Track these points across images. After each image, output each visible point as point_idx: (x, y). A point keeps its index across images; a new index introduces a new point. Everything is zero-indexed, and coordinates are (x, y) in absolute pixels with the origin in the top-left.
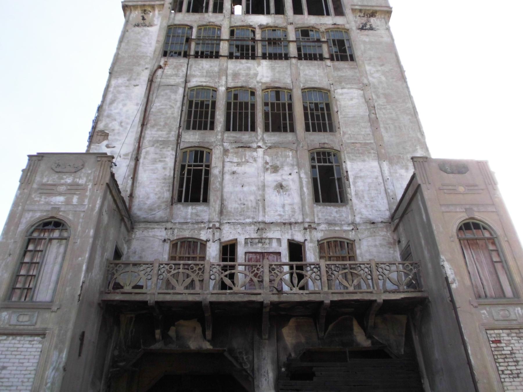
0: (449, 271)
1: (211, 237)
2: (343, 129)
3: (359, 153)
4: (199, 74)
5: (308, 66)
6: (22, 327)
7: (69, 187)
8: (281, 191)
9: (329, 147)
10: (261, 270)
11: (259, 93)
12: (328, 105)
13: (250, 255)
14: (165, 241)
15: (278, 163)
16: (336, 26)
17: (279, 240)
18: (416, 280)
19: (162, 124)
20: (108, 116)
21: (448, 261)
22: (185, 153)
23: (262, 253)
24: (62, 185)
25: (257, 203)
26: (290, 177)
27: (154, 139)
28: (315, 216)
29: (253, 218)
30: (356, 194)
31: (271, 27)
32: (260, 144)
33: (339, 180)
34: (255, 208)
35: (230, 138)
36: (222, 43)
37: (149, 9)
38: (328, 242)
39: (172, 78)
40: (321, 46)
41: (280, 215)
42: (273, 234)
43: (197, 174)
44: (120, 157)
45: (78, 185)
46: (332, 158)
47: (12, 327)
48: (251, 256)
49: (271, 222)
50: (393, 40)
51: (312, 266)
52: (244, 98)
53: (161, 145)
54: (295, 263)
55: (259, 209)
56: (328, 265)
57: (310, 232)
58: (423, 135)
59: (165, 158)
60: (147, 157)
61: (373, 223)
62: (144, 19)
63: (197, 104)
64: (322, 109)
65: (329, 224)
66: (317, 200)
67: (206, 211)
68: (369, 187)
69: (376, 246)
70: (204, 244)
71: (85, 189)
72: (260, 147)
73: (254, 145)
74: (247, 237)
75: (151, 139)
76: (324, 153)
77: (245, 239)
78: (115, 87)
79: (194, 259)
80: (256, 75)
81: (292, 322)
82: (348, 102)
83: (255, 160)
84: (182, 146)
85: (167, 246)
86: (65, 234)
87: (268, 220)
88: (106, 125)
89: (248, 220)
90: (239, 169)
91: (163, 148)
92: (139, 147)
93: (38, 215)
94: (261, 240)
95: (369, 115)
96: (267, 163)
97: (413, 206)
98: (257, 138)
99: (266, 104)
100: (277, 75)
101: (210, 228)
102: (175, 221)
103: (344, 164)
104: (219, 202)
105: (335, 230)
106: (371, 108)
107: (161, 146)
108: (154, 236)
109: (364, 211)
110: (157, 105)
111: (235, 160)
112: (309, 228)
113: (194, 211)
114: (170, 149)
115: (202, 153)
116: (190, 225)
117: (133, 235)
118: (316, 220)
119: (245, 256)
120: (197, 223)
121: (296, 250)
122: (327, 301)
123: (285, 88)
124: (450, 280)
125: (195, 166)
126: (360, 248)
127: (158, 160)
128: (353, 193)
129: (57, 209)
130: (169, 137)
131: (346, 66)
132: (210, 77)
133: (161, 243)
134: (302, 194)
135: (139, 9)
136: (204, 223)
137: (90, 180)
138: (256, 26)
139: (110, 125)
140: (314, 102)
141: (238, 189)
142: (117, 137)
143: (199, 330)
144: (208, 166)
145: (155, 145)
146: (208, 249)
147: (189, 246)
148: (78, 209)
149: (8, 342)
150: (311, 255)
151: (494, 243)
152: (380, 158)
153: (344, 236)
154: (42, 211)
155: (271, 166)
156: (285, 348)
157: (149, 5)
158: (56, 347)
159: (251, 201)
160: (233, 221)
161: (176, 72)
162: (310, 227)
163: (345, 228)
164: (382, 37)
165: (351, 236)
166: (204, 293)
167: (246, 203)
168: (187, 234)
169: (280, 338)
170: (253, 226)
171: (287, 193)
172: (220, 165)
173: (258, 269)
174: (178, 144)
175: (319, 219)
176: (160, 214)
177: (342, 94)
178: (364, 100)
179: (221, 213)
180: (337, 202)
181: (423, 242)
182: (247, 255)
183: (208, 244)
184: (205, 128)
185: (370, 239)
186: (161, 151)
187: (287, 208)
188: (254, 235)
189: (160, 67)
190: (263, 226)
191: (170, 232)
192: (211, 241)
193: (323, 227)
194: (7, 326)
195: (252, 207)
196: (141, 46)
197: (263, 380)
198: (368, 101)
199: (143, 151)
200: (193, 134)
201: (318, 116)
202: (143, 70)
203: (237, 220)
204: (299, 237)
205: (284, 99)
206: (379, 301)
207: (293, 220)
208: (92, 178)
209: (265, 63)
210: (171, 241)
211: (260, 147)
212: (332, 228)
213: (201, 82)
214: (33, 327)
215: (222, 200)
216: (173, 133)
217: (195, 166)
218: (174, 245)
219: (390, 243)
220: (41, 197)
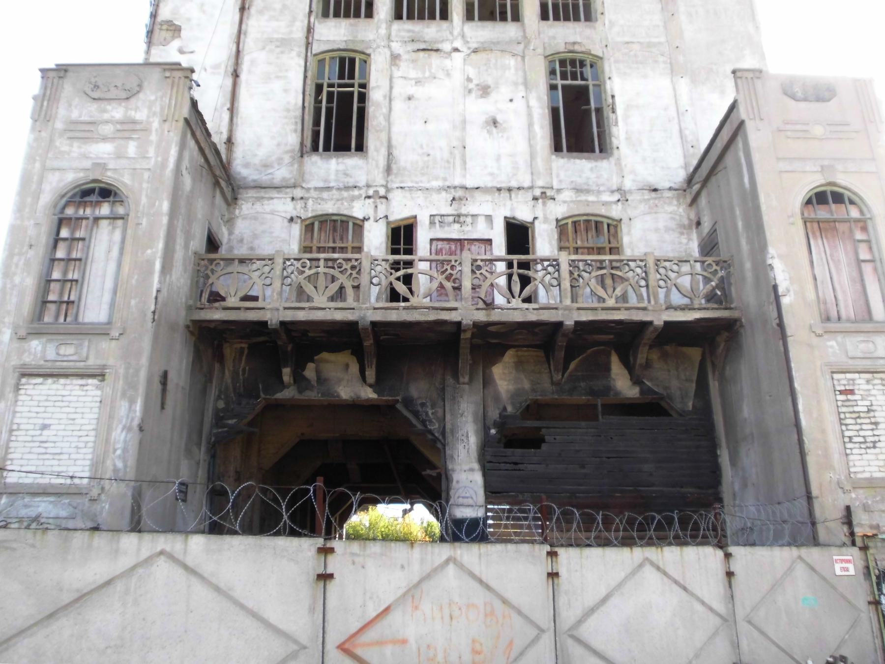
0: (781, 275)
1: (370, 212)
2: (609, 16)
6: (65, 364)
7: (119, 127)
8: (494, 130)
9: (583, 49)
10: (459, 268)
13: (440, 243)
14: (291, 220)
15: (490, 81)
17: (489, 218)
18: (723, 289)
19: (278, 6)
21: (780, 257)
22: (321, 62)
23: (460, 240)
24: (107, 122)
25: (451, 153)
28: (554, 175)
29: (445, 179)
30: (628, 139)
32: (458, 44)
33: (599, 111)
34: (448, 162)
35: (403, 34)
38: (574, 223)
41: (491, 174)
42: (478, 206)
43: (345, 99)
44: (206, 70)
45: (134, 122)
46: (588, 71)
47: (49, 364)
48: (440, 245)
49: (476, 186)
51: (546, 263)
53: (277, 47)
54: (516, 258)
55: (454, 163)
56: (573, 261)
57: (544, 204)
59: (287, 71)
61: (655, 190)
65: (578, 190)
66: (557, 148)
69: (657, 230)
70: (359, 226)
71: (147, 130)
72: (456, 50)
73: (447, 47)
76: (573, 62)
77: (431, 216)
79: (343, 250)
81: (509, 356)
83: (448, 75)
84: (316, 48)
85: (296, 229)
86: (121, 210)
87: (470, 183)
89: (436, 184)
91: (282, 52)
92: (238, 52)
94: (458, 218)
96: (469, 80)
97: (729, 159)
98: (451, 33)
101: (369, 197)
102: (309, 186)
103: (608, 82)
104: (384, 151)
105: (587, 201)
107: (278, 50)
108: (272, 213)
111: (413, 74)
112: (542, 198)
113: (341, 167)
114: (294, 54)
115: (352, 61)
116: (334, 192)
117: (237, 212)
118: (556, 185)
119: (431, 245)
120: (347, 188)
121: (518, 236)
122: (569, 323)
124: (781, 290)
125: (340, 86)
126: (629, 233)
130: (291, 32)
133: (286, 223)
134: (531, 139)
136: (360, 188)
137: (155, 114)
143: (355, 368)
144: (363, 86)
145: (267, 48)
146: (366, 233)
147: (335, 230)
148: (138, 166)
149: (46, 387)
150: (544, 243)
151: (864, 229)
152: (674, 70)
153: (603, 211)
154: (76, 170)
155: (478, 85)
156: (497, 398)
158: (124, 395)
159: (441, 149)
160: (410, 185)
162: (544, 196)
163: (606, 197)
165: (615, 212)
166: (361, 309)
167: (431, 152)
168: (329, 208)
169: (488, 381)
170: (444, 194)
172: (385, 84)
173: (452, 267)
174: (308, 45)
175: (560, 181)
176: (281, 173)
179: (388, 170)
180: (593, 151)
181: (740, 224)
182: (434, 243)
183: (367, 225)
184: (357, 15)
185: (648, 218)
186: (278, 58)
188: (447, 210)
190: (461, 194)
191: (300, 204)
192: (372, 219)
193: (567, 195)
194: (42, 362)
195: (442, 159)
197: (460, 447)
200: (335, 26)
203: (417, 183)
204: (523, 214)
206: (656, 323)
207: (514, 184)
210: (303, 221)
211: (456, 50)
212: (583, 197)
214: (82, 364)
215: (390, 147)
217: (340, 86)
218: (308, 228)
219: (683, 226)
220: (72, 146)
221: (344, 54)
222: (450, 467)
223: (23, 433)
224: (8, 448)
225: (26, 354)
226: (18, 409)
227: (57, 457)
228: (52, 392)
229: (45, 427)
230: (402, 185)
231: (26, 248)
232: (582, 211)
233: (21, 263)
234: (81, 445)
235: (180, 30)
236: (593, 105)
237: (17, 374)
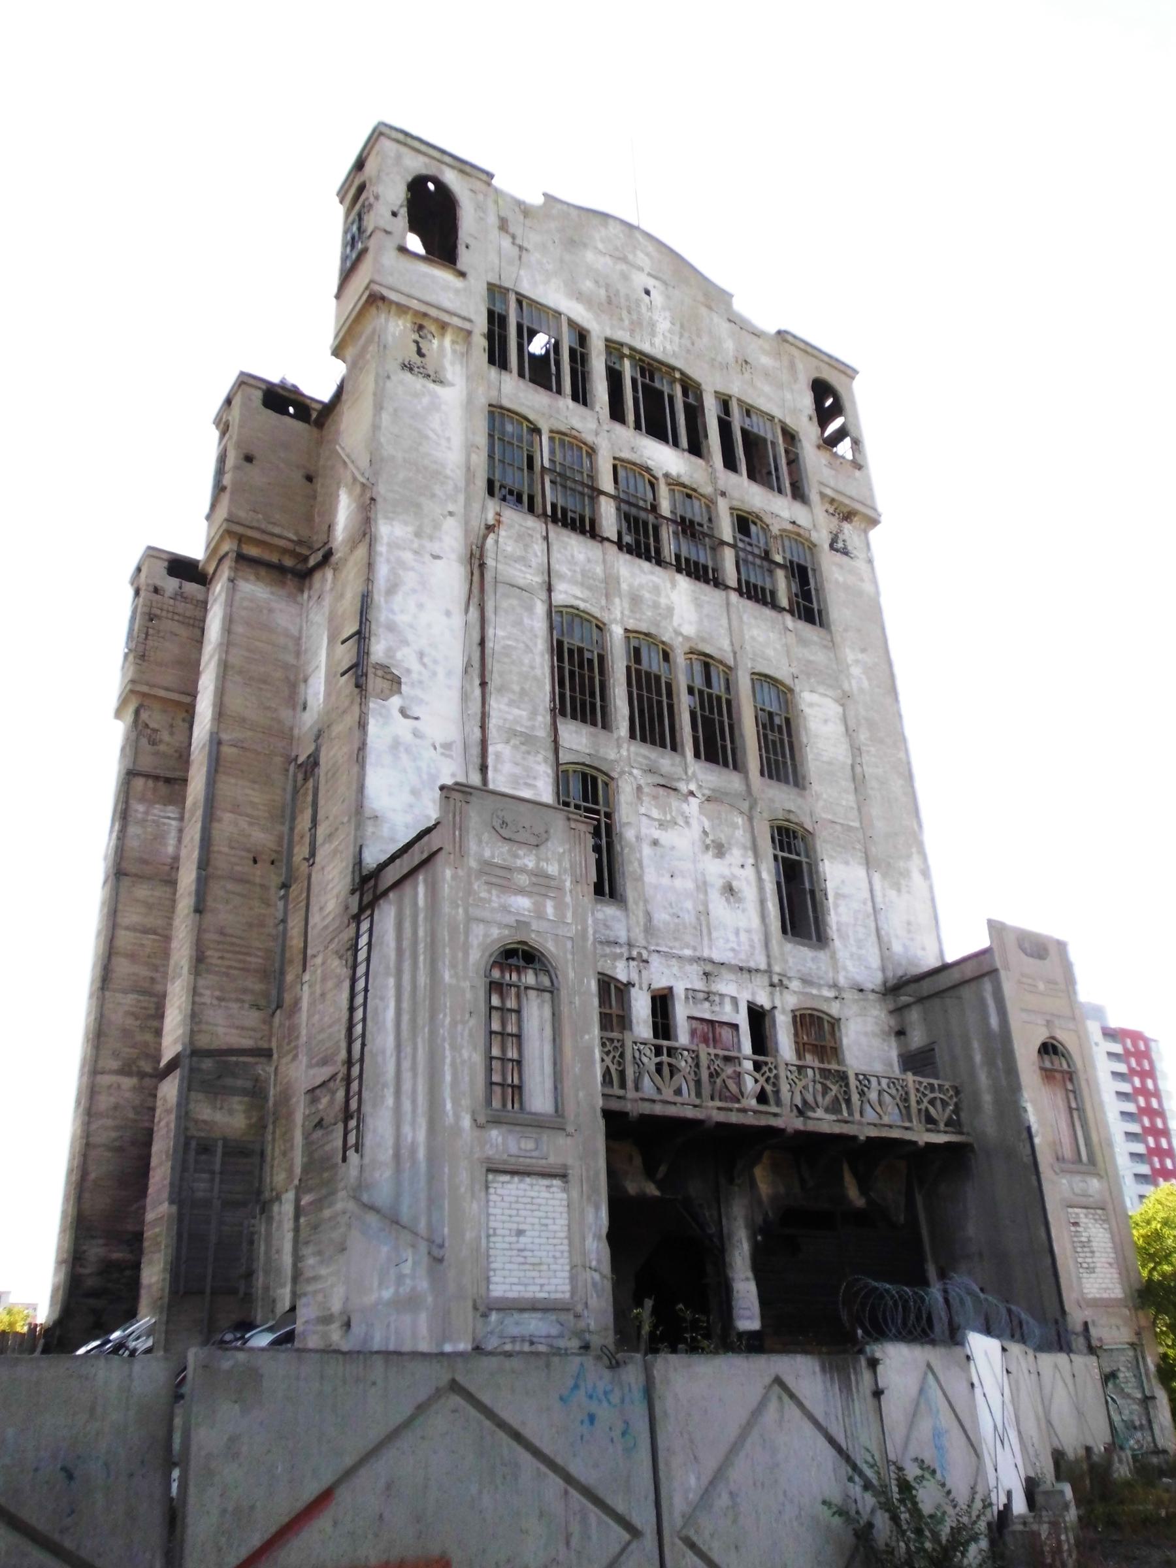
0: (1032, 1118)
2: (816, 787)
3: (839, 846)
4: (569, 574)
5: (756, 618)
6: (528, 1160)
7: (534, 879)
8: (732, 899)
9: (796, 820)
10: (775, 1072)
11: (680, 660)
12: (788, 721)
15: (723, 839)
16: (795, 529)
19: (516, 688)
20: (391, 627)
21: (1032, 1102)
25: (698, 919)
26: (741, 871)
27: (507, 726)
29: (695, 949)
30: (838, 930)
31: (685, 486)
32: (693, 787)
33: (812, 892)
34: (695, 928)
35: (640, 759)
36: (603, 500)
37: (433, 328)
39: (517, 566)
40: (771, 572)
41: (733, 950)
42: (727, 986)
44: (435, 748)
45: (547, 877)
47: (513, 1160)
52: (652, 662)
53: (522, 744)
58: (920, 826)
59: (535, 778)
60: (499, 766)
61: (861, 990)
62: (420, 353)
63: (571, 651)
64: (780, 727)
67: (619, 920)
68: (856, 919)
69: (866, 1034)
72: (692, 793)
73: (683, 787)
74: (689, 986)
75: (501, 723)
76: (787, 830)
78: (389, 545)
80: (670, 610)
81: (766, 1158)
82: (821, 724)
83: (687, 823)
87: (717, 956)
88: (390, 652)
89: (688, 952)
90: (665, 837)
91: (529, 753)
93: (495, 932)
95: (853, 767)
96: (705, 833)
98: (686, 773)
99: (691, 691)
100: (706, 623)
101: (633, 959)
103: (821, 864)
106: (856, 750)
107: (524, 748)
109: (849, 964)
110: (500, 633)
111: (655, 814)
114: (540, 758)
123: (721, 662)
126: (847, 1035)
127: (521, 781)
128: (834, 927)
129: (522, 925)
130: (533, 728)
131: (815, 638)
132: (590, 588)
134: (763, 916)
135: (409, 317)
136: (621, 946)
137: (565, 871)
138: (659, 475)
139: (399, 655)
140: (768, 709)
141: (666, 880)
142: (417, 692)
144: (608, 815)
145: (512, 742)
148: (560, 933)
149: (513, 1186)
151: (1071, 1080)
152: (869, 863)
153: (825, 1008)
154: (501, 926)
155: (713, 841)
156: (760, 1202)
157: (436, 320)
158: (589, 1198)
159: (688, 912)
161: (523, 554)
164: (862, 580)
165: (834, 1009)
166: (707, 1107)
167: (681, 914)
169: (753, 1184)
170: (695, 966)
171: (741, 906)
173: (770, 1070)
177: (811, 705)
178: (842, 729)
180: (810, 938)
181: (978, 1058)
183: (634, 991)
185: (859, 1019)
186: (524, 758)
187: (743, 937)
188: (699, 985)
189: (490, 528)
190: (711, 969)
192: (637, 986)
194: (505, 1157)
196: (427, 437)
197: (737, 1253)
198: (849, 732)
199: (491, 749)
200: (576, 732)
201: (774, 742)
202: (444, 517)
203: (671, 948)
204: (763, 1000)
205: (718, 688)
207: (752, 965)
208: (568, 866)
209: (683, 581)
211: (692, 793)
212: (808, 990)
213: (577, 598)
214: (544, 1161)
216: (540, 718)
220: (490, 892)
221: (588, 770)
222: (730, 1275)
223: (499, 1239)
224: (488, 1256)
225: (488, 1146)
226: (491, 1211)
227: (537, 1268)
228: (521, 1193)
229: (520, 1233)
230: (658, 948)
231: (467, 1016)
232: (808, 1006)
233: (466, 1033)
234: (558, 1254)
235: (400, 683)
236: (807, 886)
237: (484, 1170)
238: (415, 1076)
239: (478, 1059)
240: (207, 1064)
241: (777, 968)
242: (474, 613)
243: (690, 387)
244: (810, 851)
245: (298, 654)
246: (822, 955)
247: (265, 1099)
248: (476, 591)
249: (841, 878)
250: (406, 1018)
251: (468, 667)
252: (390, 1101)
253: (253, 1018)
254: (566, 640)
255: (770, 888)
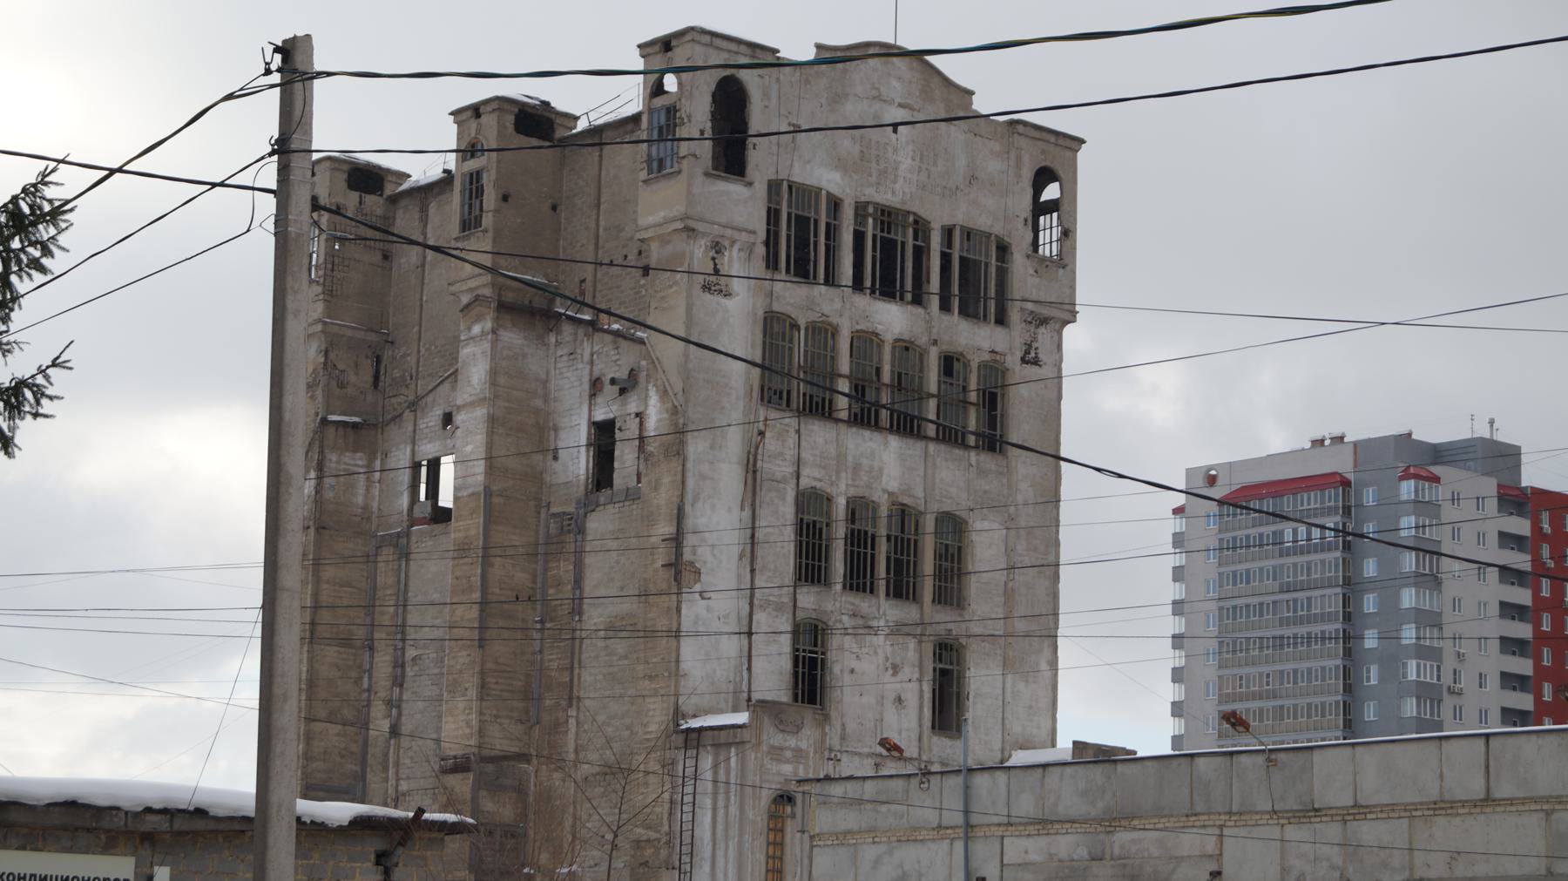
12: (960, 548)
33: (958, 694)
43: (813, 661)
50: (1060, 397)
71: (807, 757)
82: (986, 547)
89: (866, 750)
131: (993, 467)
134: (920, 718)
187: (904, 734)
209: (894, 442)
238: (727, 862)
239: (763, 858)
240: (490, 768)
241: (924, 758)
242: (747, 513)
243: (921, 227)
244: (960, 661)
245: (546, 398)
246: (959, 743)
247: (527, 794)
248: (750, 495)
249: (982, 679)
250: (720, 828)
251: (741, 557)
252: (707, 868)
253: (518, 729)
254: (806, 517)
255: (928, 696)
